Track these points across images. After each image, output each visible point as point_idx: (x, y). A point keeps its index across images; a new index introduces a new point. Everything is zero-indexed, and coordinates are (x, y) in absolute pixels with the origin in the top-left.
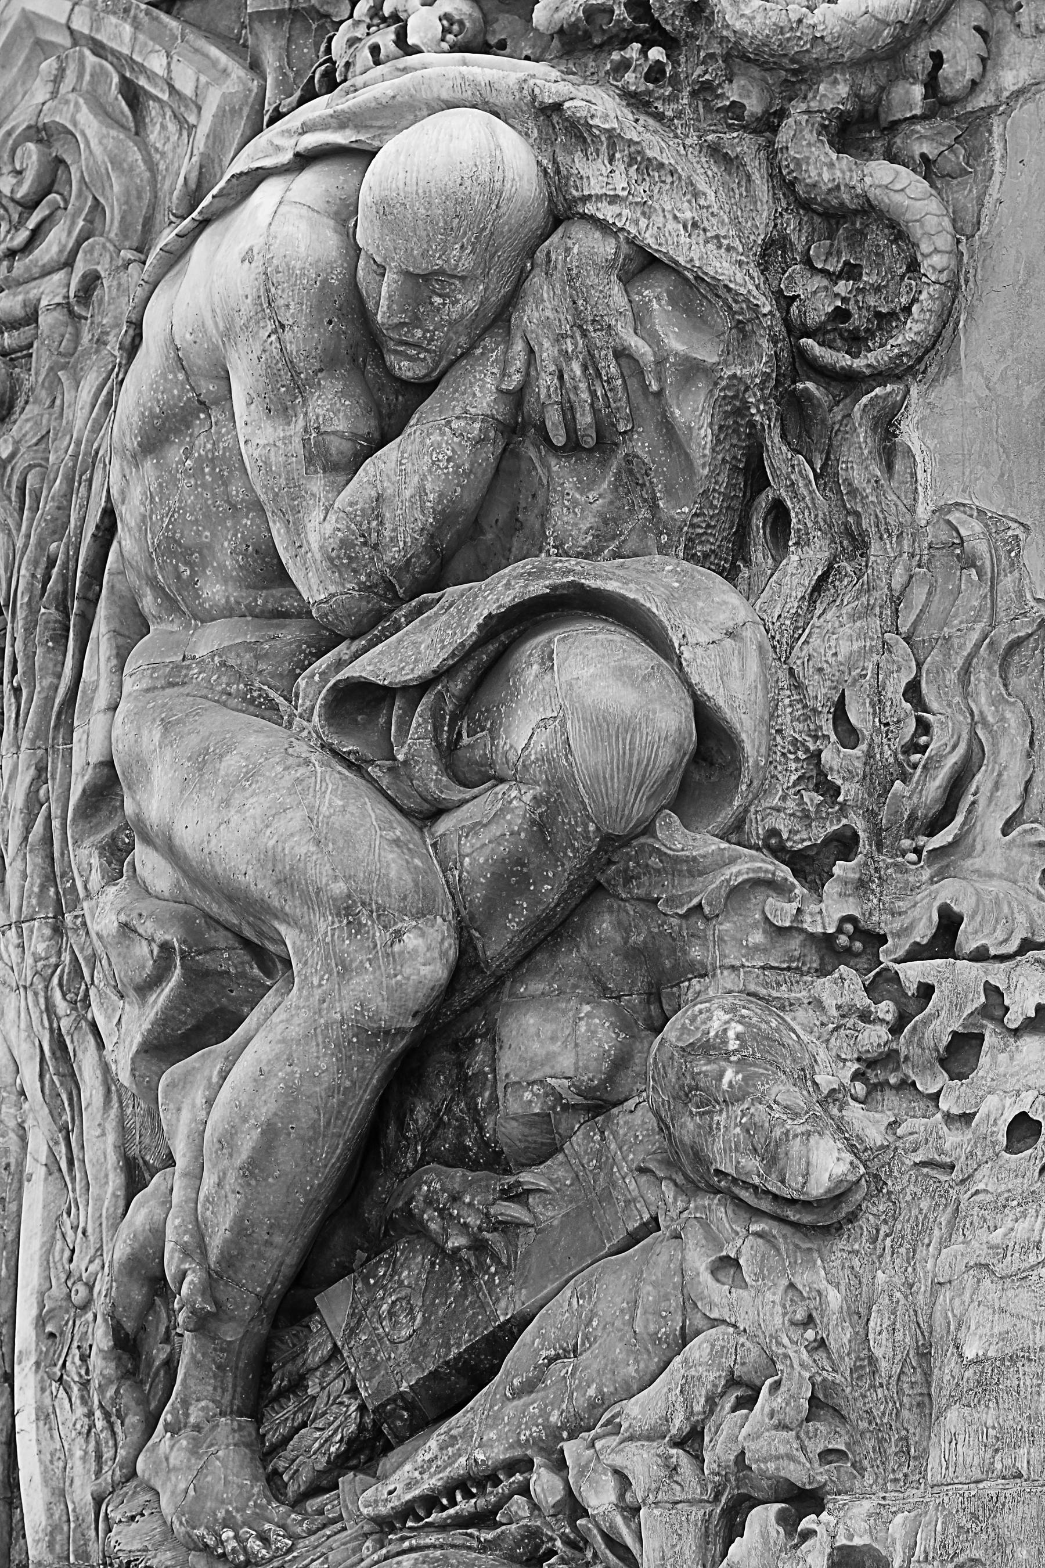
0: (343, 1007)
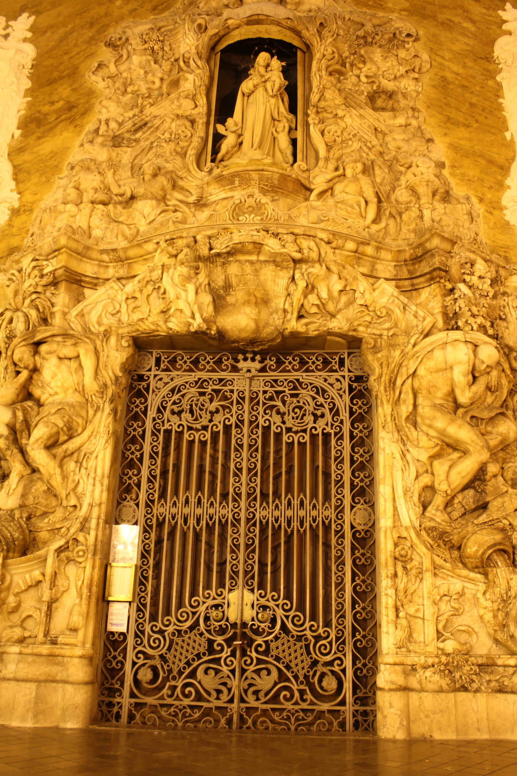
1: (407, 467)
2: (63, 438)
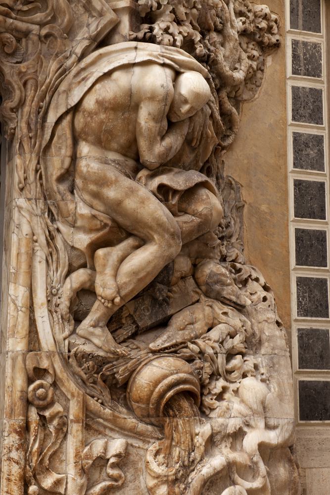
0: (167, 254)
1: (55, 257)
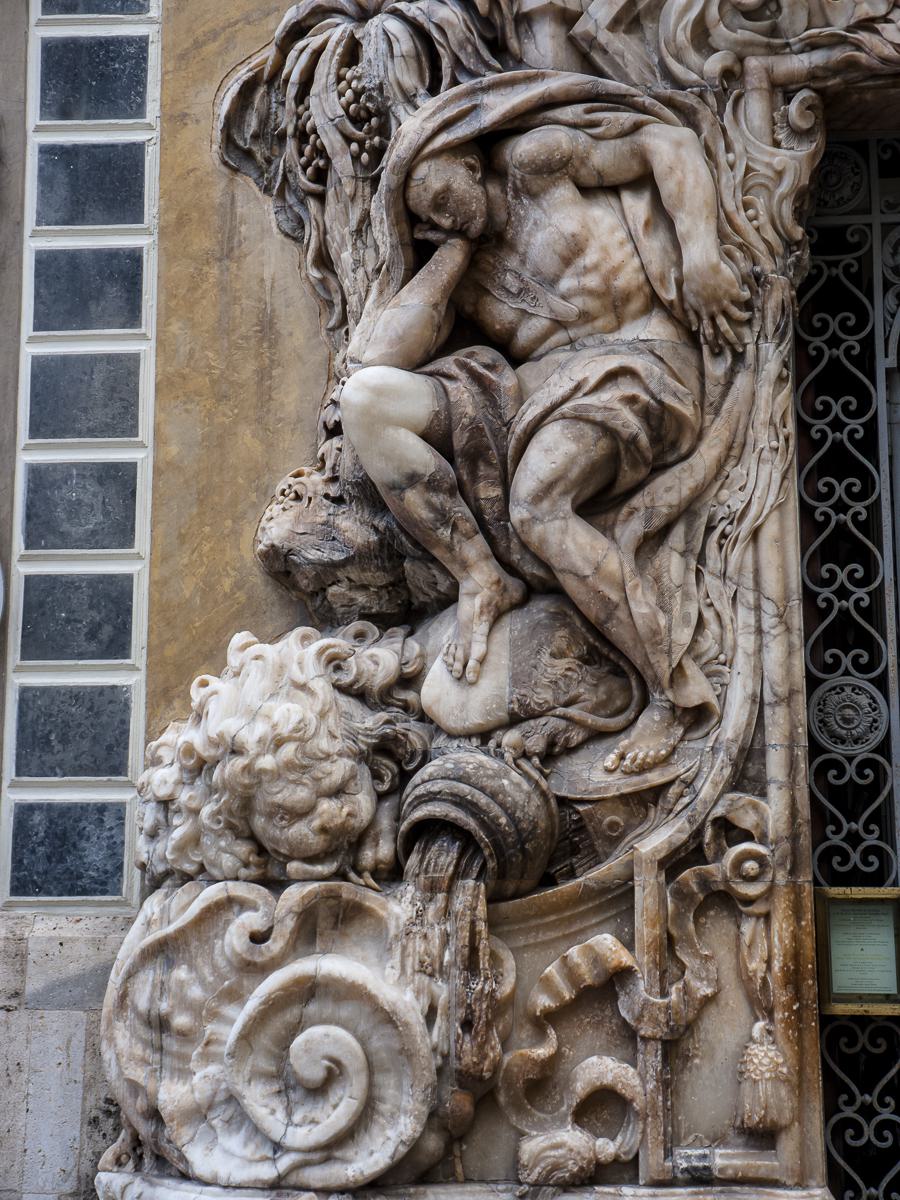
2: (628, 476)
